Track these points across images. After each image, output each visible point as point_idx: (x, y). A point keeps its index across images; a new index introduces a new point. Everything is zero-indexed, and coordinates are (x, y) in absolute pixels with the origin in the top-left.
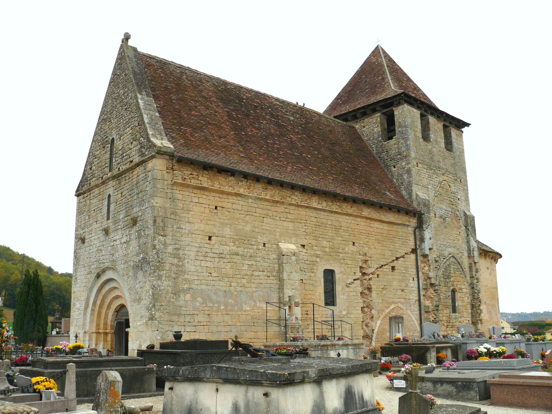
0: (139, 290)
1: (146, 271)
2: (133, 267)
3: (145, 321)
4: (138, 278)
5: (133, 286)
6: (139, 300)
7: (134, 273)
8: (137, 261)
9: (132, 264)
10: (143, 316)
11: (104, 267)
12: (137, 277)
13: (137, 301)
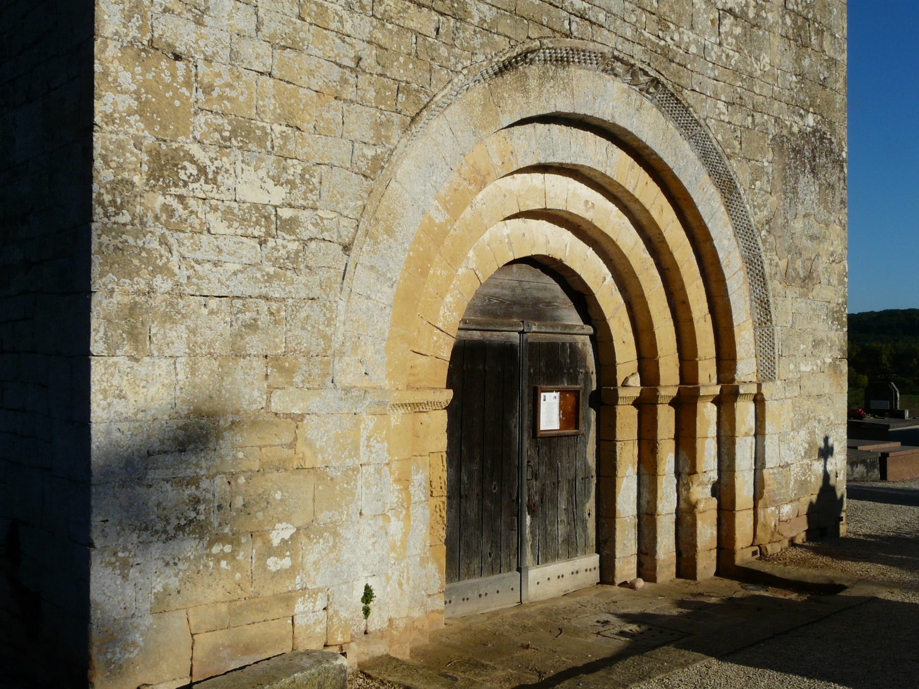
0: (809, 243)
1: (831, 186)
2: (779, 143)
3: (829, 360)
4: (801, 196)
5: (780, 221)
6: (808, 279)
7: (784, 169)
8: (795, 129)
9: (773, 130)
10: (822, 341)
11: (591, 46)
12: (795, 191)
13: (799, 281)
